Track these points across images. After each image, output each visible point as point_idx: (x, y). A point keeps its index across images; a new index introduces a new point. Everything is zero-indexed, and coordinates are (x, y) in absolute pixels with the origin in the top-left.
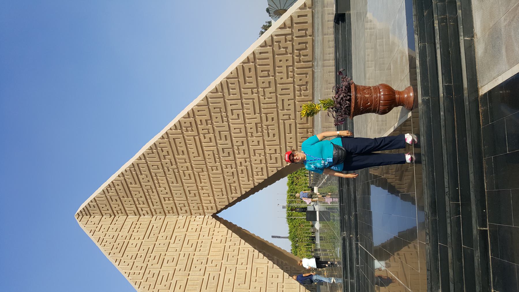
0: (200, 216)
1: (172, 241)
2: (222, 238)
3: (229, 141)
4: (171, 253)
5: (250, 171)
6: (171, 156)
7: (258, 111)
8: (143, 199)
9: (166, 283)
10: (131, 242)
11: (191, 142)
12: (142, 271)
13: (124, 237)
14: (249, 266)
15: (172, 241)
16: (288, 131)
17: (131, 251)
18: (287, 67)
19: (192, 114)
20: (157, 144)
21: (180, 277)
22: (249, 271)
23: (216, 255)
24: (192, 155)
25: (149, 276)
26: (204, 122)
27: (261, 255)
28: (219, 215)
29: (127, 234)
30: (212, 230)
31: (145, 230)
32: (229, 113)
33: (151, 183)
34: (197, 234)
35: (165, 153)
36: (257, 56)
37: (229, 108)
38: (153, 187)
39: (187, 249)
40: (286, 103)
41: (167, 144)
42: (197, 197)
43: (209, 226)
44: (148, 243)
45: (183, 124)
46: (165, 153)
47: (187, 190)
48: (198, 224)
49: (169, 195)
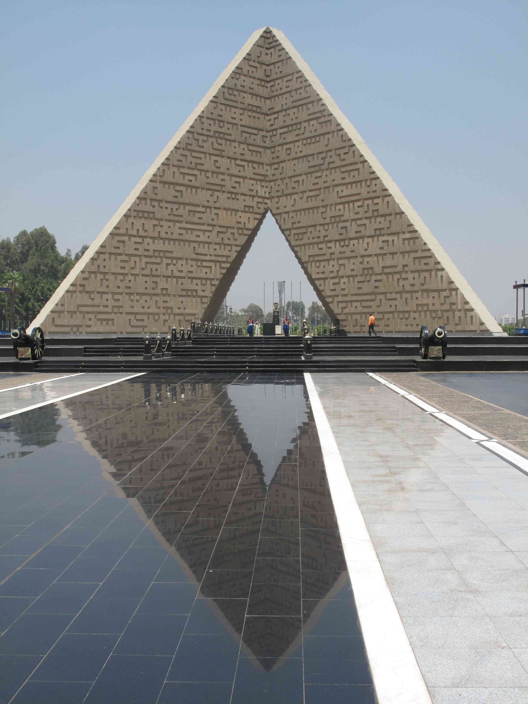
0: (267, 193)
1: (238, 162)
2: (243, 223)
3: (353, 235)
4: (224, 163)
5: (321, 258)
6: (338, 163)
7: (387, 270)
8: (289, 122)
9: (193, 163)
10: (238, 111)
11: (355, 190)
12: (205, 132)
13: (243, 100)
14: (213, 258)
15: (238, 162)
16: (364, 304)
17: (227, 115)
18: (427, 305)
19: (385, 194)
20: (353, 149)
21: (201, 180)
22: (208, 258)
23: (225, 218)
24: (340, 189)
25: (200, 141)
26: (375, 208)
27: (224, 271)
28: (269, 215)
29: (246, 104)
30: (251, 210)
31: (252, 125)
32: (385, 238)
33: (307, 134)
34: (246, 191)
35: (343, 156)
36: (440, 273)
37: (390, 238)
38: (302, 137)
39: (229, 183)
40: (393, 303)
41: (352, 160)
42: (291, 191)
43: (255, 205)
44: (235, 134)
45: (374, 182)
46: (343, 156)
47: (300, 179)
48: (259, 192)
49: (293, 155)
